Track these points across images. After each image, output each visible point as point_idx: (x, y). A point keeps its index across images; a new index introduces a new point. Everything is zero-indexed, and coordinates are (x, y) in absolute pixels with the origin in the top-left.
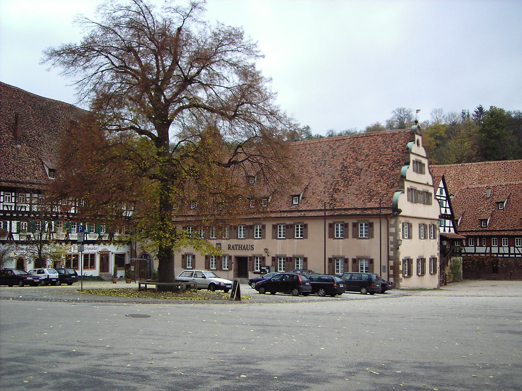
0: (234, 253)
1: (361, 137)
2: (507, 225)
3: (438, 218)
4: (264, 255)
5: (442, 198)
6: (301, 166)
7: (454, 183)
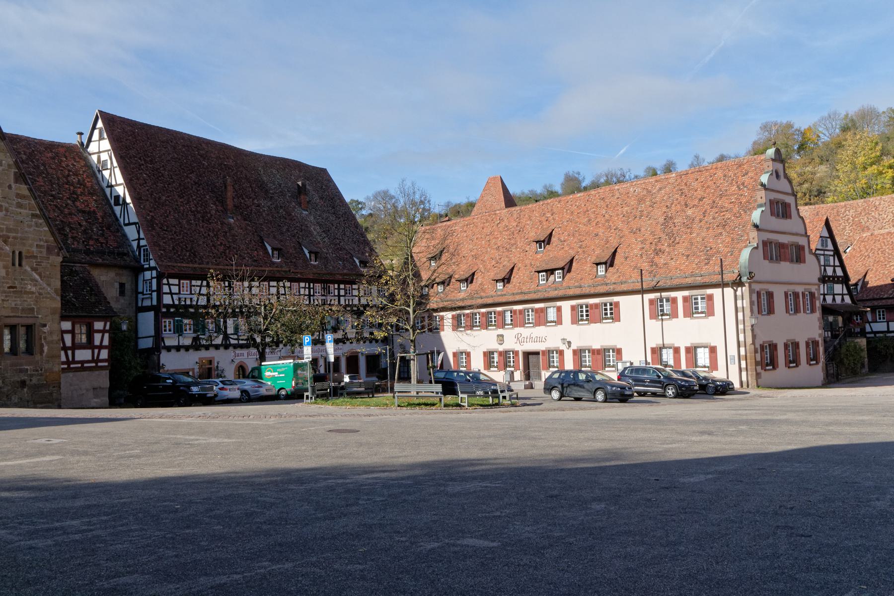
0: (521, 348)
1: (692, 173)
3: (817, 281)
4: (563, 347)
5: (826, 253)
6: (607, 221)
7: (854, 228)
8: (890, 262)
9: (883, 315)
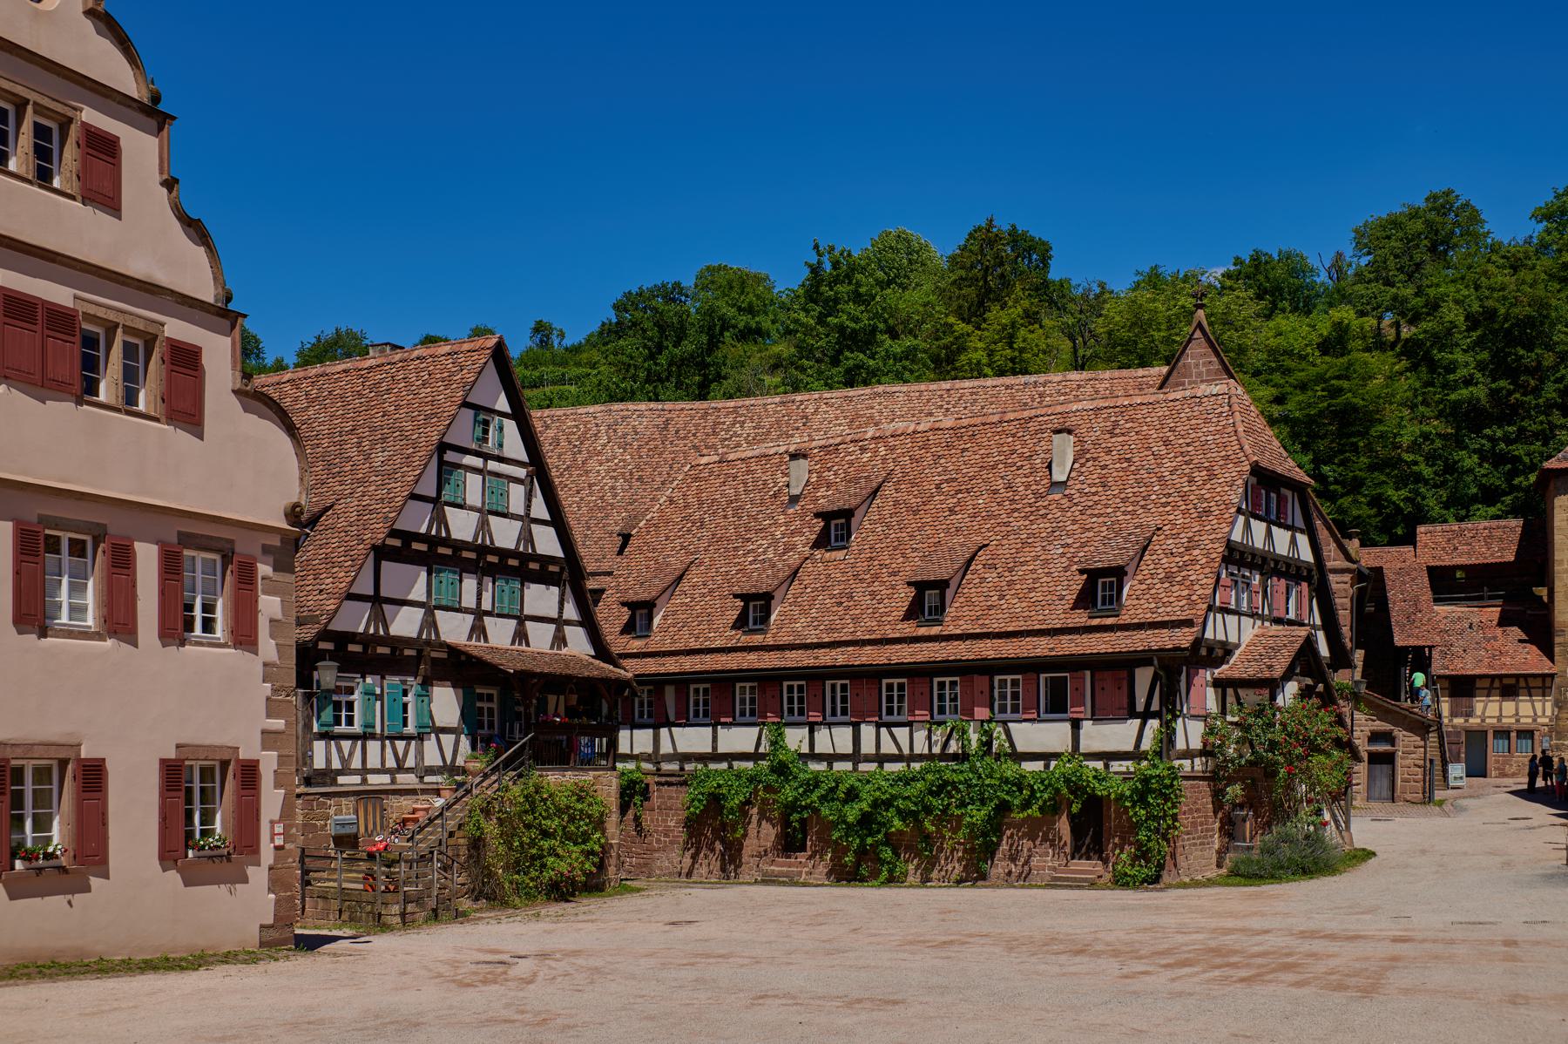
2: (855, 619)
8: (749, 540)
9: (706, 703)
